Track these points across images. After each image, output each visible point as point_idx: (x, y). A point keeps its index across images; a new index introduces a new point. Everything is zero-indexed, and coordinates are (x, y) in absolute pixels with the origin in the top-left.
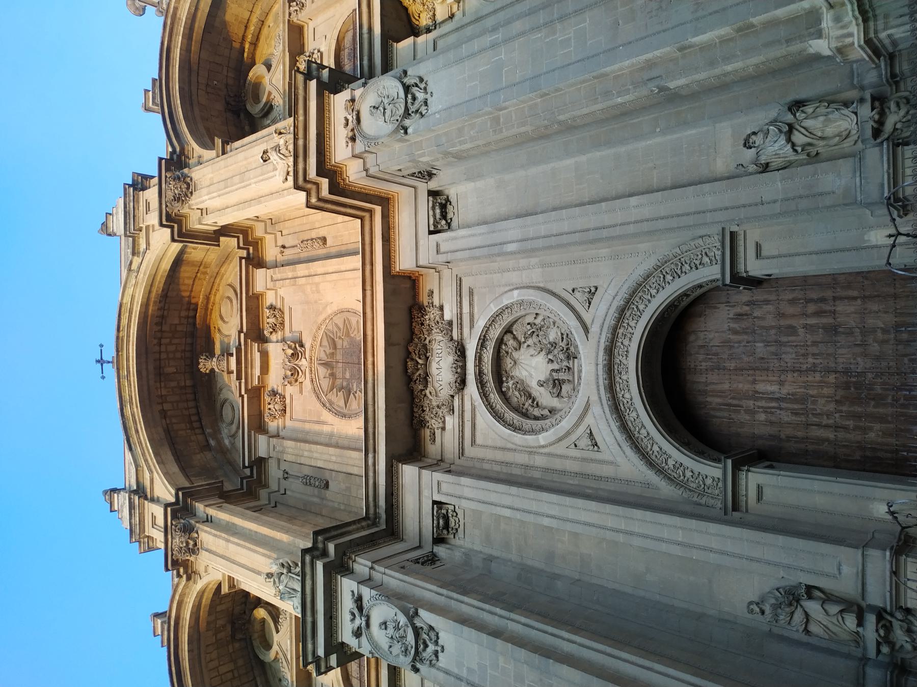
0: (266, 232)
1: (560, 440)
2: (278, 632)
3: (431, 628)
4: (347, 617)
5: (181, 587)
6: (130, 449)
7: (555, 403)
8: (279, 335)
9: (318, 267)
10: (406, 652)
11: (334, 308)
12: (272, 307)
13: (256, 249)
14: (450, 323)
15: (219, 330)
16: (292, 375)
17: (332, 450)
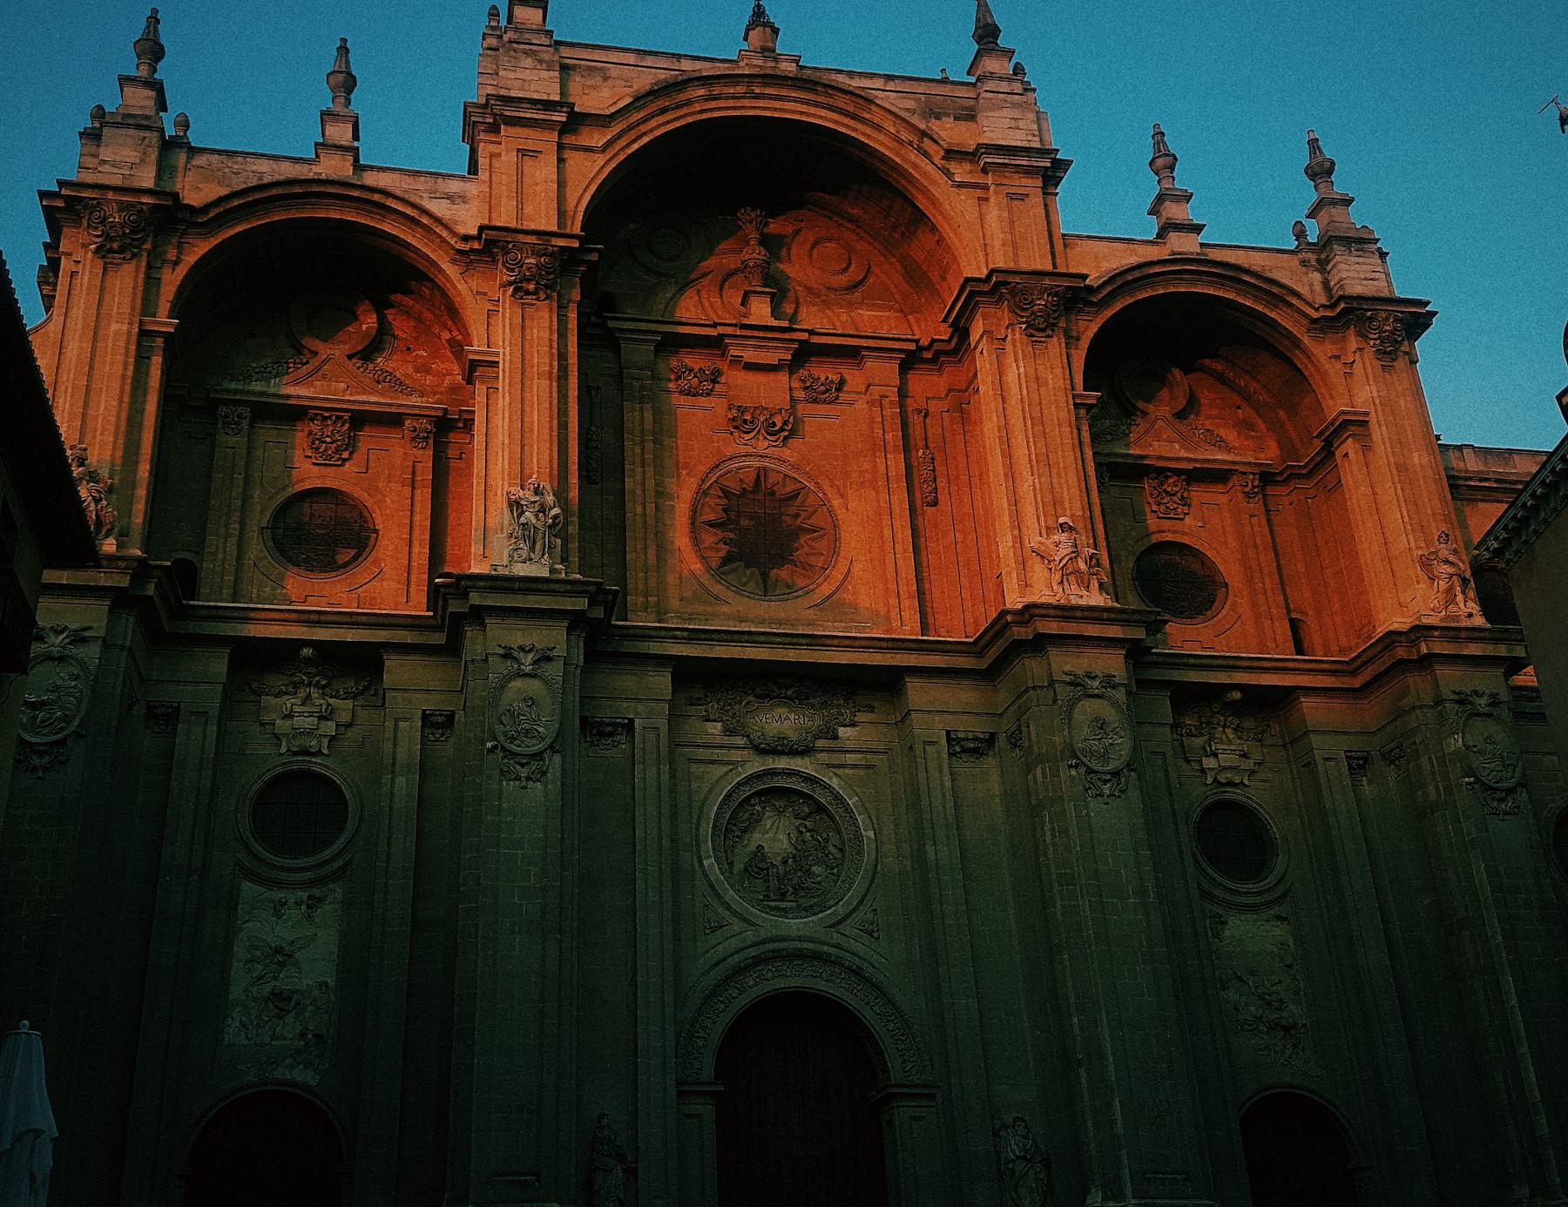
0: (950, 390)
1: (712, 887)
2: (350, 357)
3: (544, 773)
4: (527, 643)
5: (445, 234)
6: (637, 99)
7: (739, 866)
8: (800, 394)
9: (900, 500)
10: (513, 739)
11: (841, 514)
12: (842, 382)
13: (927, 361)
14: (836, 737)
15: (797, 232)
16: (745, 421)
17: (651, 508)
